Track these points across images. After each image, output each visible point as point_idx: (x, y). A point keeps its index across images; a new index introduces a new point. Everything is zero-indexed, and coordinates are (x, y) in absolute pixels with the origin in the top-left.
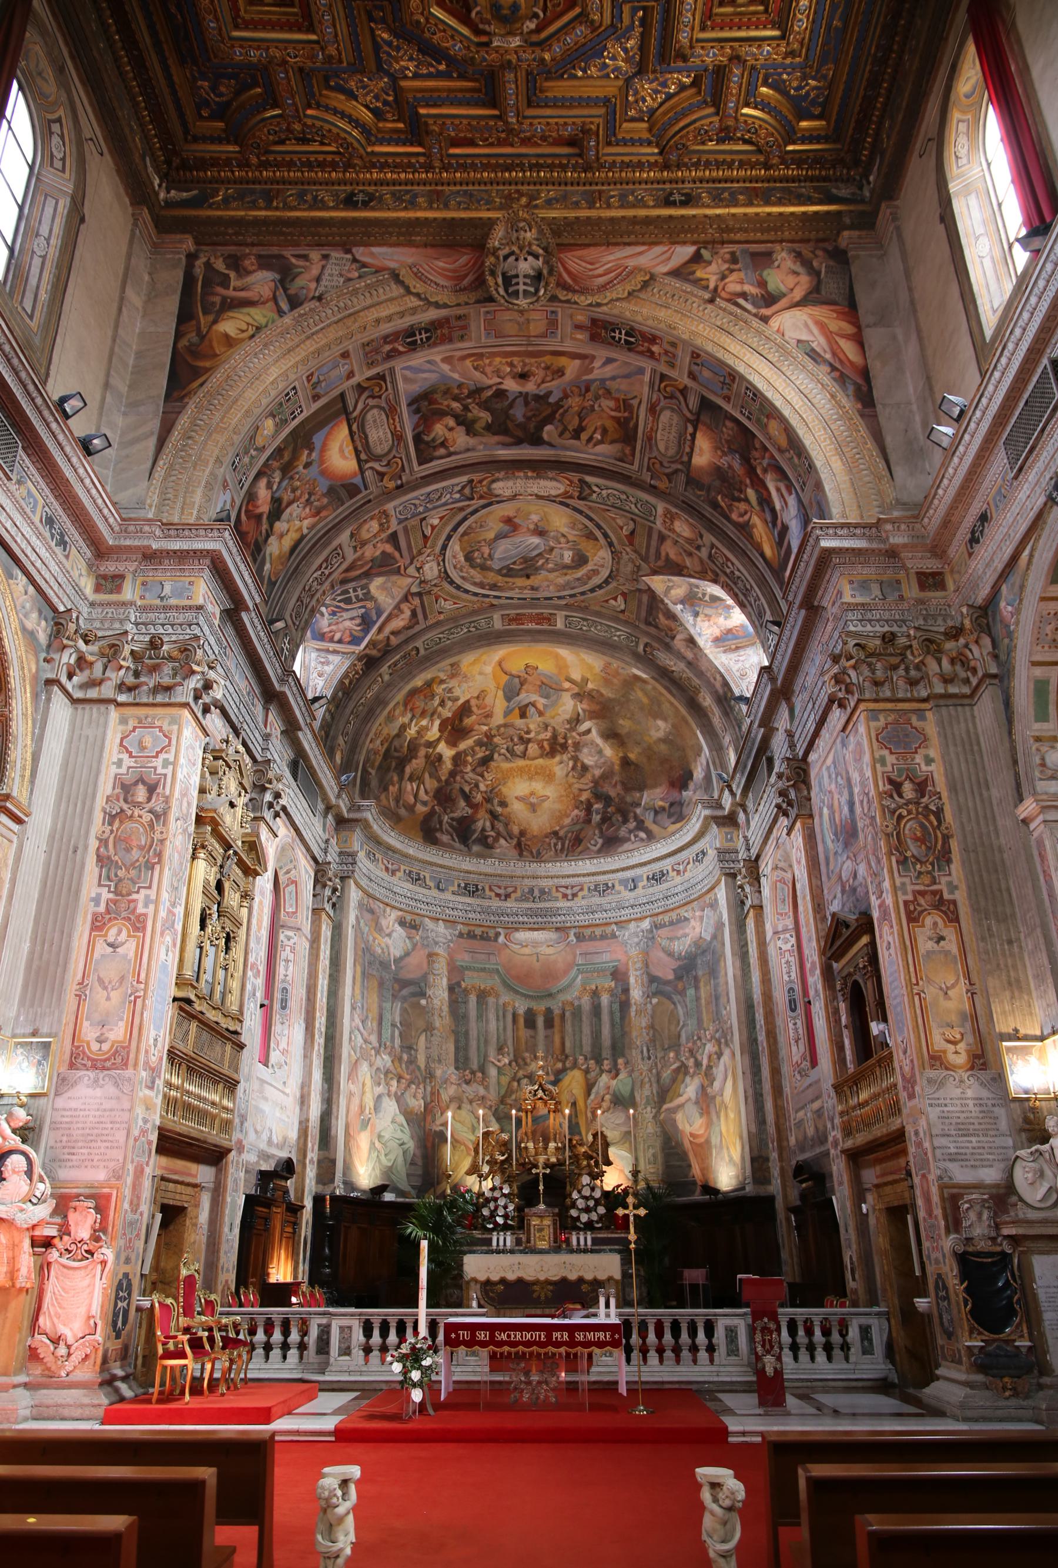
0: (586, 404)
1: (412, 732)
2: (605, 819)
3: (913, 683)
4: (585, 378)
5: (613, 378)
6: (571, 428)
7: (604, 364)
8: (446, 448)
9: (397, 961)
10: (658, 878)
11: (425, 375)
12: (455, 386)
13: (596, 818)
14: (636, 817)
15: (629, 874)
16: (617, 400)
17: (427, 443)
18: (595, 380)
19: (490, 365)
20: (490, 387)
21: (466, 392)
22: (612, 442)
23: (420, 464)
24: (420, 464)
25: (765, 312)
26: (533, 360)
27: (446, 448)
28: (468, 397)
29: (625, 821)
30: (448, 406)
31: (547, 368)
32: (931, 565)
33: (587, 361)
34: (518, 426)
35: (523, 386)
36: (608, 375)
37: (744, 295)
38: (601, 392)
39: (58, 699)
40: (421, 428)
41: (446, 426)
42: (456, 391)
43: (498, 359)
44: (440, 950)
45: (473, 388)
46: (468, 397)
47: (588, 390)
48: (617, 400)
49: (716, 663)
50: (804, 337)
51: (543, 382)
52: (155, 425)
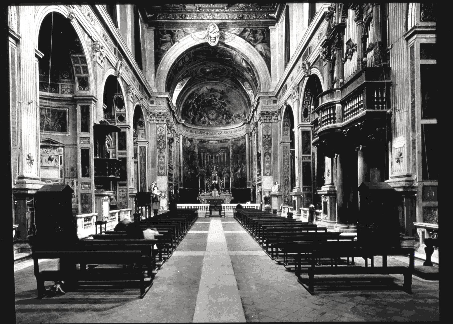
1: (190, 102)
2: (226, 118)
3: (270, 120)
9: (189, 148)
10: (235, 131)
13: (225, 118)
14: (232, 118)
15: (231, 130)
25: (255, 44)
29: (230, 119)
32: (275, 99)
37: (251, 40)
39: (149, 124)
44: (196, 145)
49: (247, 92)
50: (261, 50)
52: (154, 71)
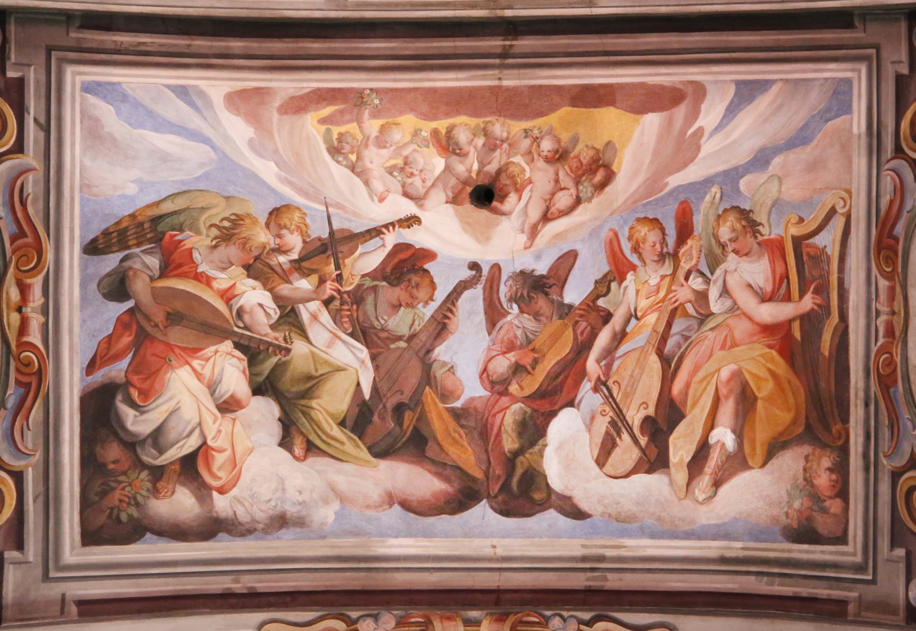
0: (683, 294)
4: (676, 180)
5: (761, 160)
6: (635, 417)
7: (732, 111)
8: (202, 490)
11: (166, 142)
12: (261, 212)
16: (775, 248)
17: (132, 444)
18: (708, 182)
19: (381, 143)
20: (375, 232)
21: (295, 242)
22: (774, 449)
23: (90, 537)
24: (90, 537)
26: (517, 127)
27: (202, 490)
28: (300, 266)
30: (228, 296)
31: (559, 156)
33: (681, 111)
34: (458, 415)
35: (483, 235)
36: (742, 156)
38: (725, 233)
40: (118, 370)
41: (212, 387)
42: (263, 237)
43: (409, 121)
45: (320, 231)
46: (300, 266)
47: (685, 231)
48: (775, 248)
51: (546, 218)
